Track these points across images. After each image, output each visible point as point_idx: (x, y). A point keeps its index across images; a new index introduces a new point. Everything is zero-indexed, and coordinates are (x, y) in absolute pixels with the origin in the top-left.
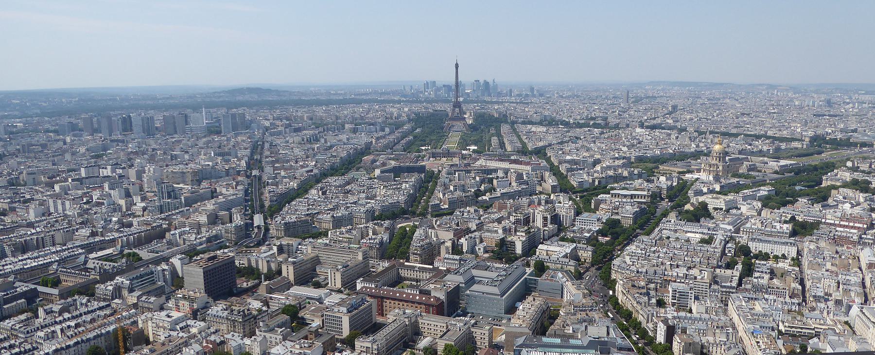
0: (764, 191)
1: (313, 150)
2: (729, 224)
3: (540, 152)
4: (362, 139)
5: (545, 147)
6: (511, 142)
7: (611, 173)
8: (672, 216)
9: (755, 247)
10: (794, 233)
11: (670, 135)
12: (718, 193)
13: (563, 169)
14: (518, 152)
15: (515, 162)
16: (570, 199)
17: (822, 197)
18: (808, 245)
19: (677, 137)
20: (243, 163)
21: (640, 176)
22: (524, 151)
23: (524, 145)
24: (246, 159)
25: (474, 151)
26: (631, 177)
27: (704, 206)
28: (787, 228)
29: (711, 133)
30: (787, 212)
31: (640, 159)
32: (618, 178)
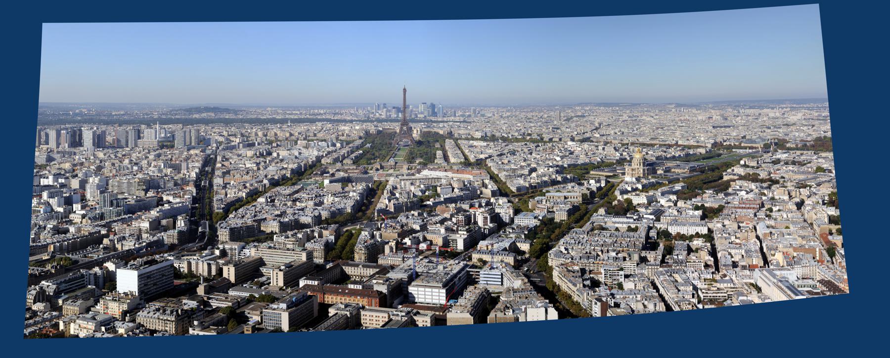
0: (678, 187)
1: (265, 162)
2: (651, 214)
3: (480, 163)
4: (312, 154)
5: (486, 158)
6: (456, 156)
7: (546, 179)
8: (602, 211)
9: (673, 230)
10: (703, 217)
11: (597, 146)
12: (642, 191)
13: (502, 176)
14: (461, 163)
15: (458, 171)
16: (509, 202)
17: (723, 188)
18: (716, 224)
19: (604, 149)
20: (193, 175)
21: (571, 181)
22: (467, 163)
23: (466, 158)
24: (197, 170)
25: (420, 163)
26: (565, 181)
27: (629, 202)
28: (699, 213)
29: (632, 144)
30: (697, 201)
31: (573, 166)
32: (554, 183)
